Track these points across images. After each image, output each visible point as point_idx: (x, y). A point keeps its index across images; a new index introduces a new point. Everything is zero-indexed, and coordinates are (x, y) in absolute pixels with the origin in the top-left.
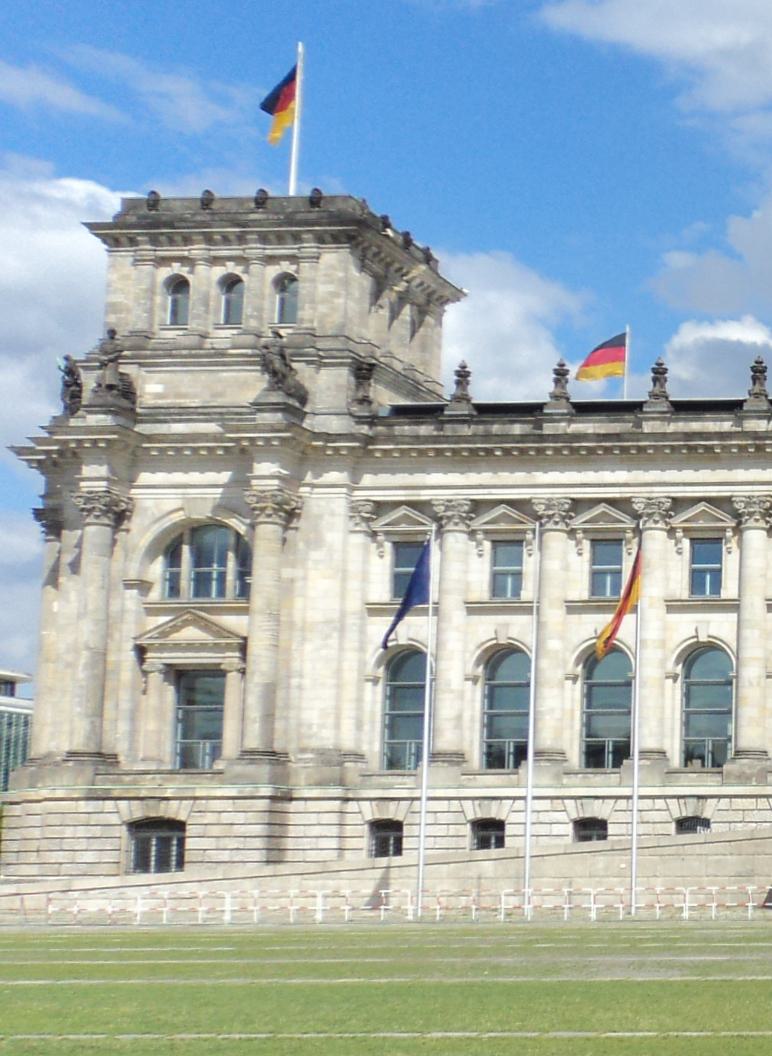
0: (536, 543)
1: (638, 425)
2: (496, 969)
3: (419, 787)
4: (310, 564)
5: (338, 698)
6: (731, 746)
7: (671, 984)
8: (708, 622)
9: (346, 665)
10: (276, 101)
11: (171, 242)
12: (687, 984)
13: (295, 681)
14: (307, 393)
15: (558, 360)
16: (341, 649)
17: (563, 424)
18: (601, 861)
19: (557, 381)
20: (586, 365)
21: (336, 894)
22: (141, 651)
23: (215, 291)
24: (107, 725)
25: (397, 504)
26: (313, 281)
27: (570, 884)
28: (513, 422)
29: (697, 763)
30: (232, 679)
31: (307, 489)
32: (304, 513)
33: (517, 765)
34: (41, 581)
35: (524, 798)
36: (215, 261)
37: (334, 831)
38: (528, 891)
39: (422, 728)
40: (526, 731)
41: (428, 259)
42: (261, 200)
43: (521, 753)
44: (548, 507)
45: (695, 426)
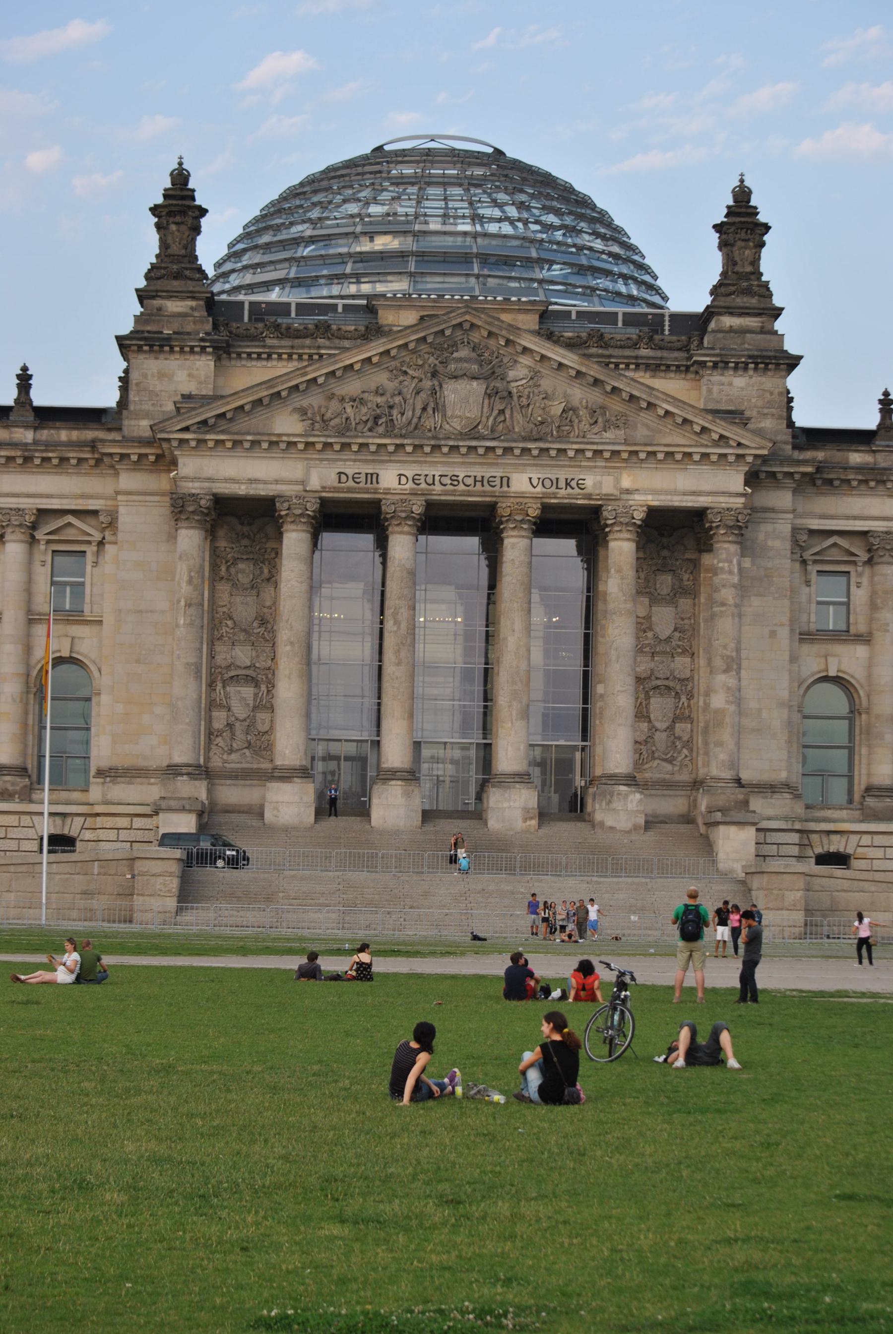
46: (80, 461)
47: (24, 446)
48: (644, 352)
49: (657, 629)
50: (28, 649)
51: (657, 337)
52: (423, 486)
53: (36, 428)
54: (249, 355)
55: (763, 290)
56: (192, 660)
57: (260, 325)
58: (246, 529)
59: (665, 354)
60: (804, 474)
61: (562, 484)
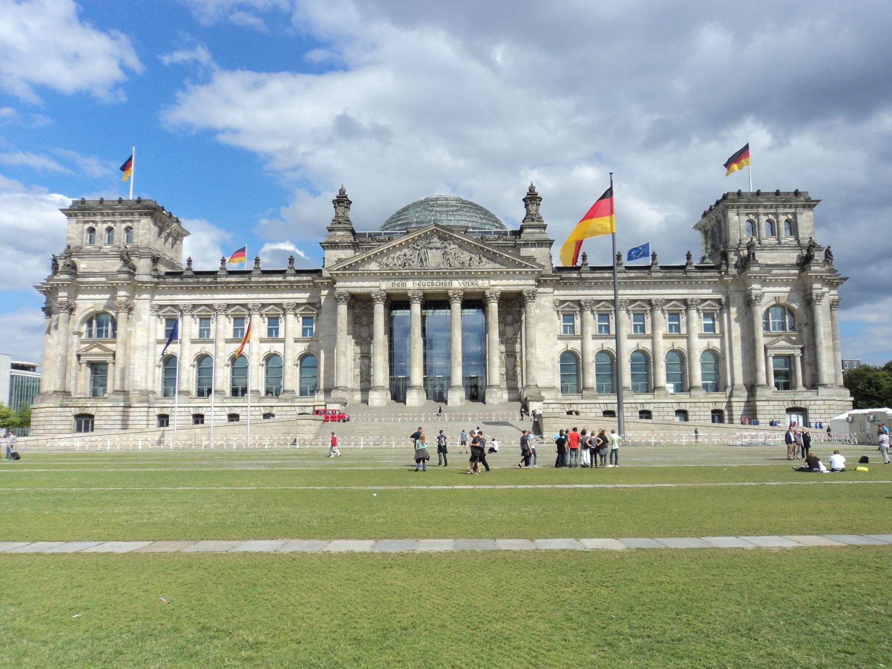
0: (215, 319)
1: (250, 278)
2: (201, 466)
3: (175, 403)
4: (137, 326)
5: (147, 373)
6: (282, 389)
7: (261, 471)
8: (274, 346)
9: (149, 361)
10: (125, 167)
11: (89, 215)
12: (267, 471)
13: (132, 367)
14: (136, 267)
15: (222, 256)
16: (148, 355)
17: (224, 278)
18: (237, 429)
19: (222, 263)
20: (232, 257)
21: (146, 440)
22: (79, 356)
23: (104, 232)
24: (67, 382)
25: (167, 306)
26: (138, 229)
27: (227, 437)
28: (207, 277)
29: (270, 395)
30: (110, 366)
31: (136, 300)
32: (135, 309)
33: (208, 395)
34: (44, 332)
35: (211, 407)
36: (104, 222)
37: (145, 418)
38: (212, 439)
39: (175, 383)
40: (212, 384)
41: (178, 221)
42: (120, 201)
43: (210, 391)
44: (219, 307)
45: (270, 279)
46: (309, 286)
47: (290, 282)
48: (499, 242)
49: (507, 335)
50: (294, 350)
51: (504, 237)
52: (422, 286)
53: (295, 276)
54: (366, 248)
55: (540, 219)
56: (343, 350)
57: (370, 239)
58: (365, 306)
59: (507, 242)
60: (556, 280)
61: (470, 284)
